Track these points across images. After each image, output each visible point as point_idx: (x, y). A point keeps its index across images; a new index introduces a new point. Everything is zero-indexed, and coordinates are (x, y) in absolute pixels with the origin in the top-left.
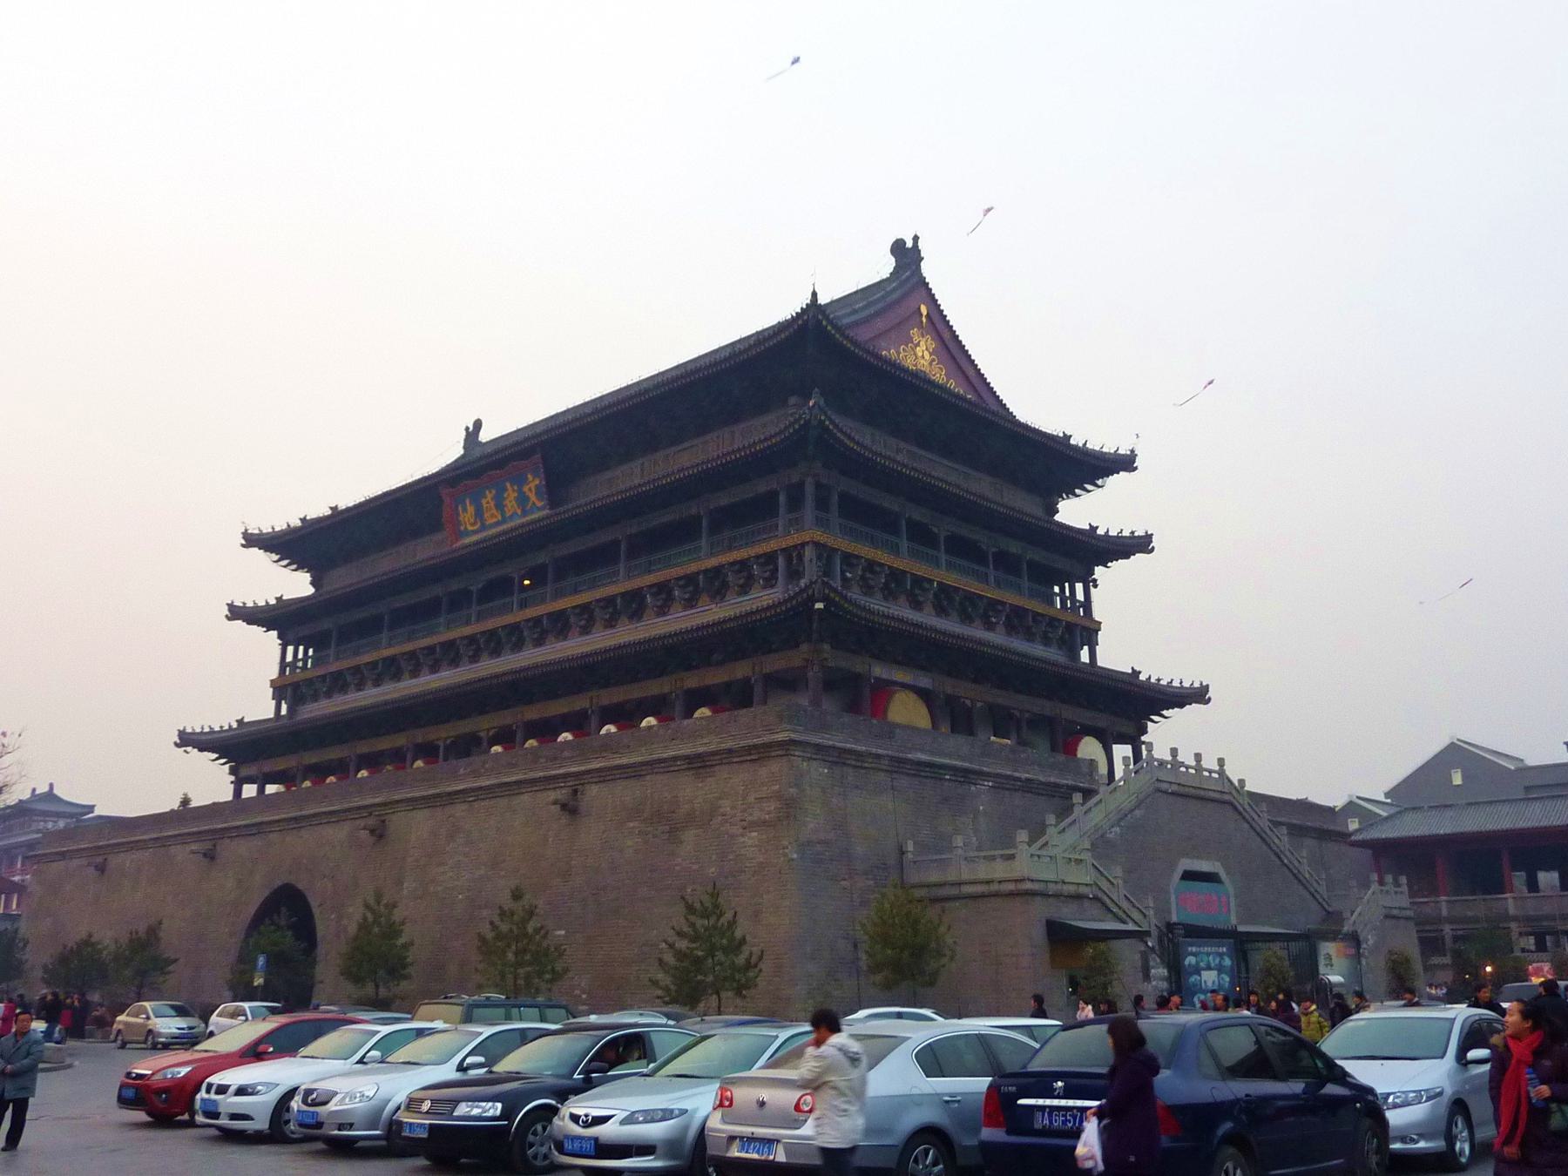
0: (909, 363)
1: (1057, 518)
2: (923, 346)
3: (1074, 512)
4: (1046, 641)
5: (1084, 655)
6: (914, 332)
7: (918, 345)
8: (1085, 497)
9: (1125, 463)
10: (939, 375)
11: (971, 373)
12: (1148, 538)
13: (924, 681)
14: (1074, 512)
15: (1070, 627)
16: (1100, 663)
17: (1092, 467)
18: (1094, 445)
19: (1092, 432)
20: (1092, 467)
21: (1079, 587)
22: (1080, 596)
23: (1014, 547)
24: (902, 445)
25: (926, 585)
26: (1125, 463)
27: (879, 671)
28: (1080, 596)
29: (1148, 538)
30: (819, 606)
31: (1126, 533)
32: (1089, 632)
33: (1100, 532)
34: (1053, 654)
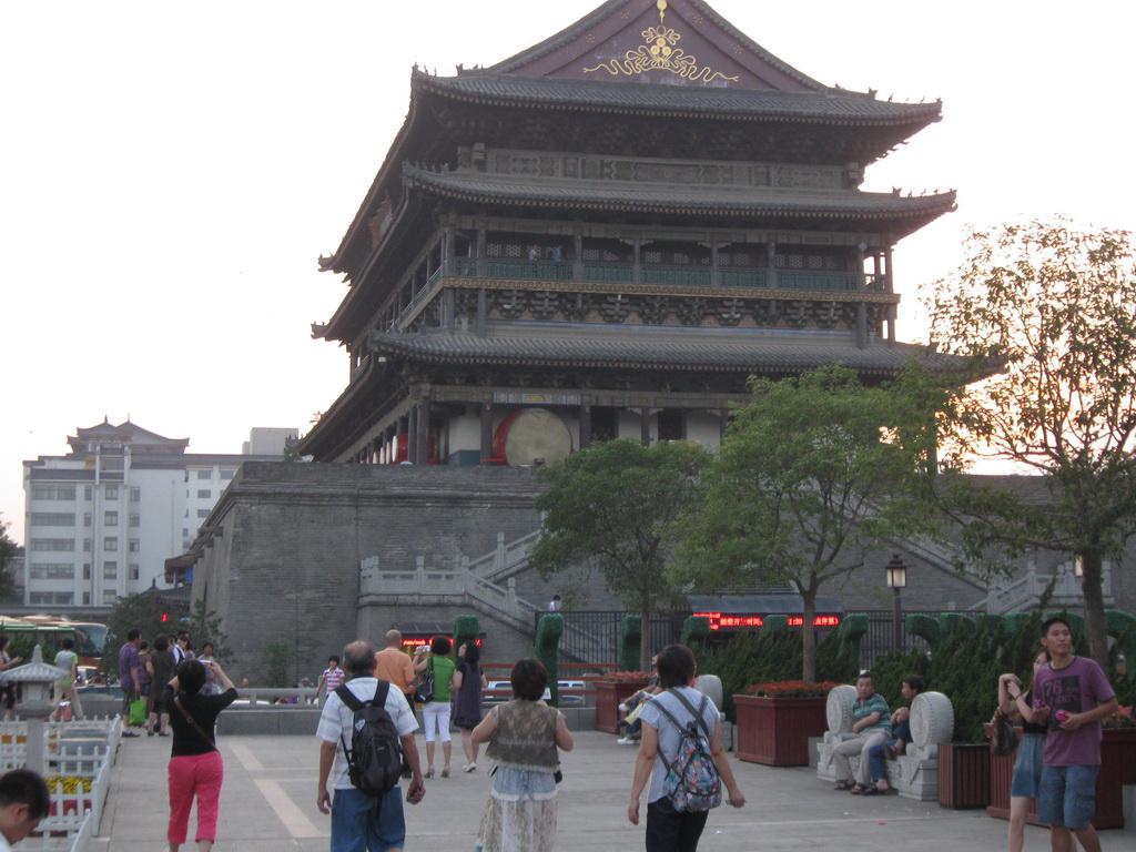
0: (639, 68)
1: (862, 188)
2: (661, 42)
3: (882, 176)
6: (649, 33)
7: (654, 43)
10: (686, 70)
11: (736, 51)
12: (951, 195)
13: (570, 398)
17: (892, 125)
18: (898, 99)
19: (897, 89)
21: (882, 260)
22: (883, 272)
23: (753, 237)
24: (608, 159)
25: (611, 300)
27: (505, 397)
28: (883, 272)
29: (951, 195)
30: (382, 359)
31: (930, 193)
33: (903, 194)
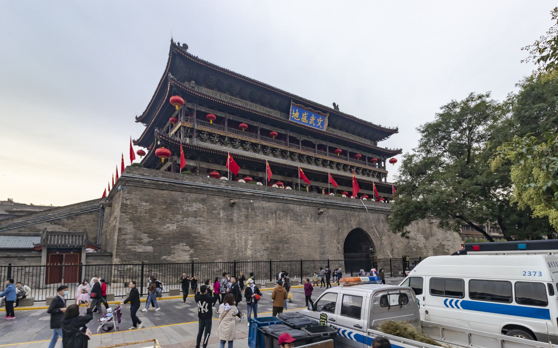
1: (378, 146)
3: (381, 144)
4: (373, 176)
5: (383, 180)
8: (384, 141)
9: (396, 131)
12: (401, 150)
14: (381, 144)
15: (379, 173)
16: (387, 181)
17: (387, 133)
18: (387, 127)
20: (387, 133)
21: (383, 163)
22: (383, 165)
26: (396, 131)
28: (383, 165)
31: (396, 149)
32: (385, 175)
34: (375, 180)
